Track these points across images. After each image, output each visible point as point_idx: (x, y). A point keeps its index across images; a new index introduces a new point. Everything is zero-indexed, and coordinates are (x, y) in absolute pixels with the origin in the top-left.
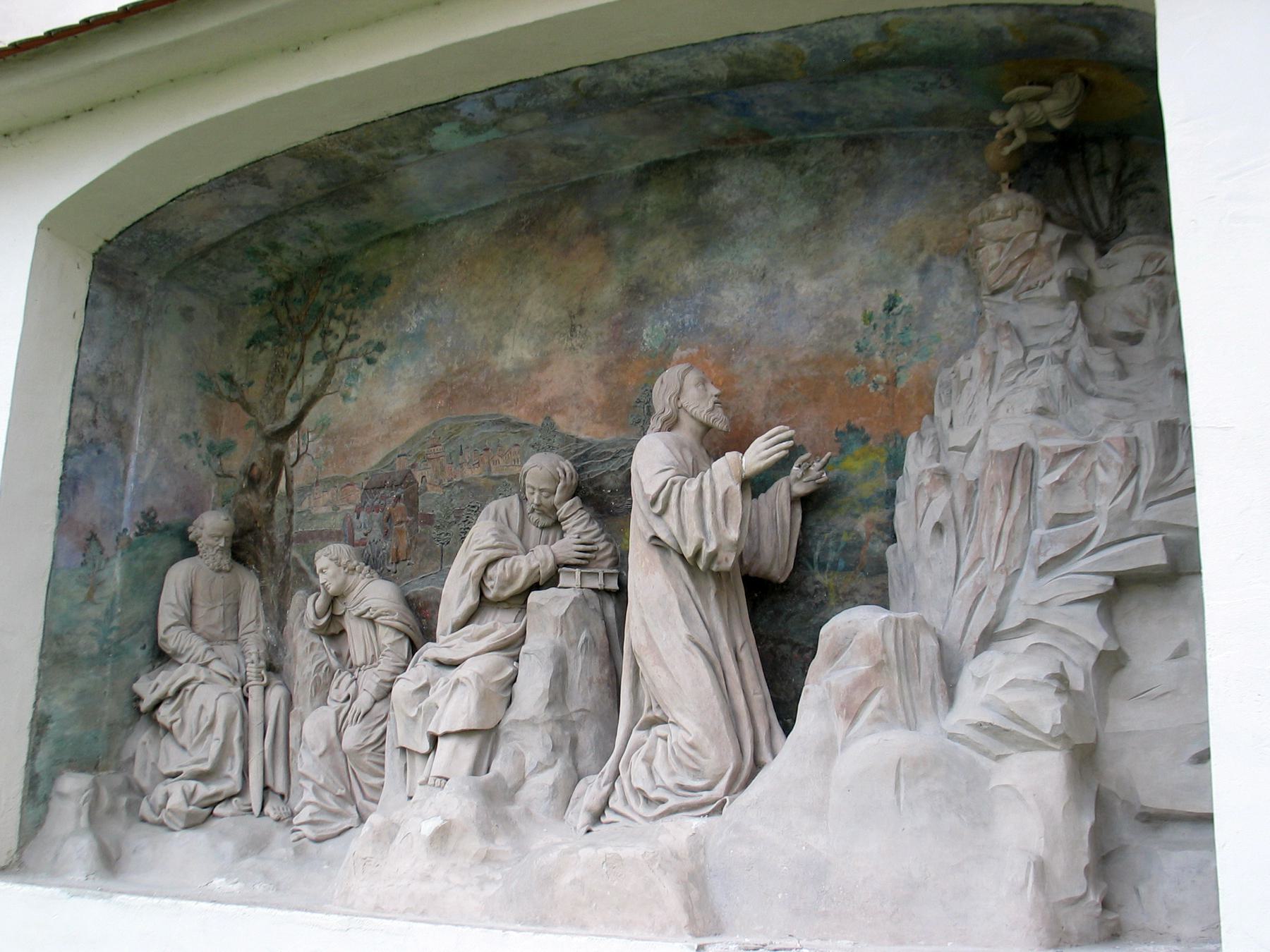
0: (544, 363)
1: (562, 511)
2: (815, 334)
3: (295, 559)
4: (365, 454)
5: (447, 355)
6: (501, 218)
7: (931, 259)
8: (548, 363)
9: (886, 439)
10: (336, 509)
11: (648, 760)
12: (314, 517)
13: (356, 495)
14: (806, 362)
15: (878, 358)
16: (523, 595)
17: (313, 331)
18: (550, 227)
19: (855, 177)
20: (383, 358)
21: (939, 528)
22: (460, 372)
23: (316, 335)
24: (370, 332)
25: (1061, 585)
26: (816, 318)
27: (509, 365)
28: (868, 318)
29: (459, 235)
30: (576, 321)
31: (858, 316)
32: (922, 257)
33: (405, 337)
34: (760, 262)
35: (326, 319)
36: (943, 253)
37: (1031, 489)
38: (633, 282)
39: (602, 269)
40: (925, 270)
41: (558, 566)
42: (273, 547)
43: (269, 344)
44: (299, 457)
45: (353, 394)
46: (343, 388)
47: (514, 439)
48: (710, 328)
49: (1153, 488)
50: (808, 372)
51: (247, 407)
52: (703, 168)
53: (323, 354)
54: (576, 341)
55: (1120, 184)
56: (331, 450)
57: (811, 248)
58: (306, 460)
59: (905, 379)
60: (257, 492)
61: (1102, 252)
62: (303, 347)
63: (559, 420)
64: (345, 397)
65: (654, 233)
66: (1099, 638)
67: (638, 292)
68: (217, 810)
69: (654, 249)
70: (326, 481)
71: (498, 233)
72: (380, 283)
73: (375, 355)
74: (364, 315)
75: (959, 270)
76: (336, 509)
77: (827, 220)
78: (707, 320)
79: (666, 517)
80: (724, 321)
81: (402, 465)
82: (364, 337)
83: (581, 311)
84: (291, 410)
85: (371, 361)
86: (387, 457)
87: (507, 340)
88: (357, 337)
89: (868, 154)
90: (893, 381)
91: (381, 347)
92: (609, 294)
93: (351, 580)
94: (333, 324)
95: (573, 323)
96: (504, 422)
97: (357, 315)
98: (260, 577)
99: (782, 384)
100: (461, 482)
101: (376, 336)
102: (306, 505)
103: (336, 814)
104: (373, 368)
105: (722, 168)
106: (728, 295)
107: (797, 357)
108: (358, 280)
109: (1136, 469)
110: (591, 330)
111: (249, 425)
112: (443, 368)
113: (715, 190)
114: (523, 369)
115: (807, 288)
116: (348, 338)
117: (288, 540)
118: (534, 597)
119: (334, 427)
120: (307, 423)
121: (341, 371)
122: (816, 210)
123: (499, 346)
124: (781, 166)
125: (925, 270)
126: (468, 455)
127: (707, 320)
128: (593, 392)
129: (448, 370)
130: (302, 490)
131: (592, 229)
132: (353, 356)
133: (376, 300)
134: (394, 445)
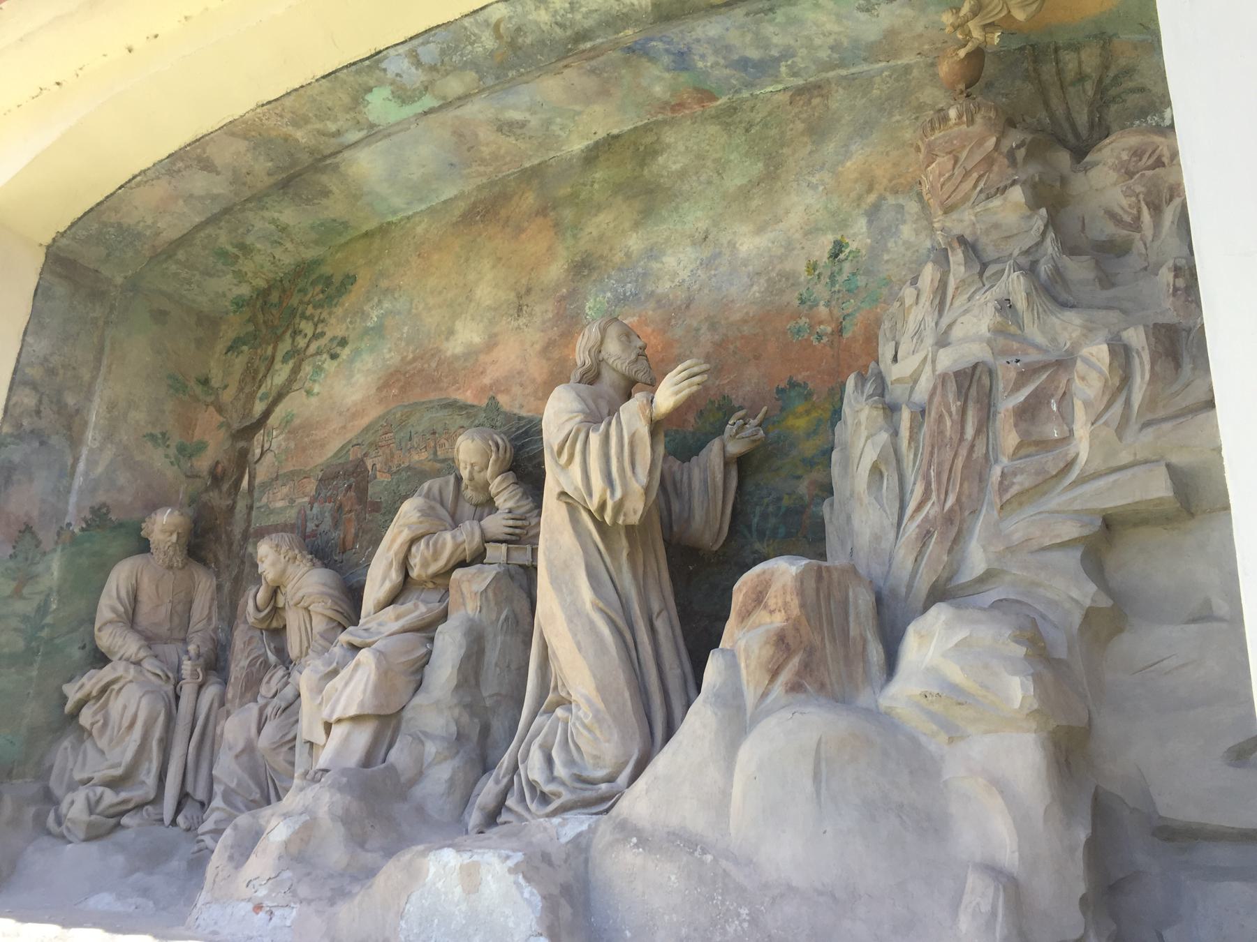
0: (491, 343)
1: (493, 489)
4: (323, 446)
7: (882, 198)
8: (496, 344)
10: (292, 501)
12: (272, 512)
13: (311, 486)
14: (745, 321)
15: (822, 310)
16: (447, 573)
17: (284, 332)
18: (503, 213)
20: (345, 353)
22: (415, 359)
23: (288, 336)
28: (812, 267)
30: (523, 302)
31: (802, 267)
32: (872, 198)
33: (366, 331)
34: (703, 225)
35: (297, 320)
36: (895, 192)
38: (578, 258)
39: (549, 248)
42: (231, 545)
43: (245, 348)
44: (262, 454)
45: (316, 389)
46: (307, 385)
49: (1151, 402)
50: (746, 330)
51: (220, 410)
54: (522, 321)
56: (292, 445)
57: (755, 203)
58: (269, 457)
62: (275, 348)
63: (503, 400)
65: (599, 208)
66: (1085, 592)
68: (125, 820)
70: (285, 475)
71: (455, 224)
73: (338, 350)
74: (330, 314)
75: (913, 207)
76: (292, 501)
77: (772, 173)
80: (664, 287)
82: (329, 335)
83: (529, 291)
84: (259, 408)
85: (334, 357)
86: (342, 448)
87: (459, 325)
88: (323, 334)
90: (840, 331)
91: (343, 342)
92: (555, 271)
96: (452, 405)
99: (720, 345)
100: (409, 468)
101: (340, 331)
102: (264, 500)
104: (335, 363)
106: (670, 261)
107: (737, 316)
108: (328, 281)
109: (1126, 380)
113: (661, 160)
114: (472, 353)
116: (316, 336)
117: (245, 536)
118: (457, 574)
119: (297, 422)
120: (273, 420)
121: (307, 368)
122: (760, 165)
123: (451, 332)
125: (873, 213)
127: (649, 288)
129: (403, 359)
131: (542, 212)
132: (319, 352)
134: (349, 436)
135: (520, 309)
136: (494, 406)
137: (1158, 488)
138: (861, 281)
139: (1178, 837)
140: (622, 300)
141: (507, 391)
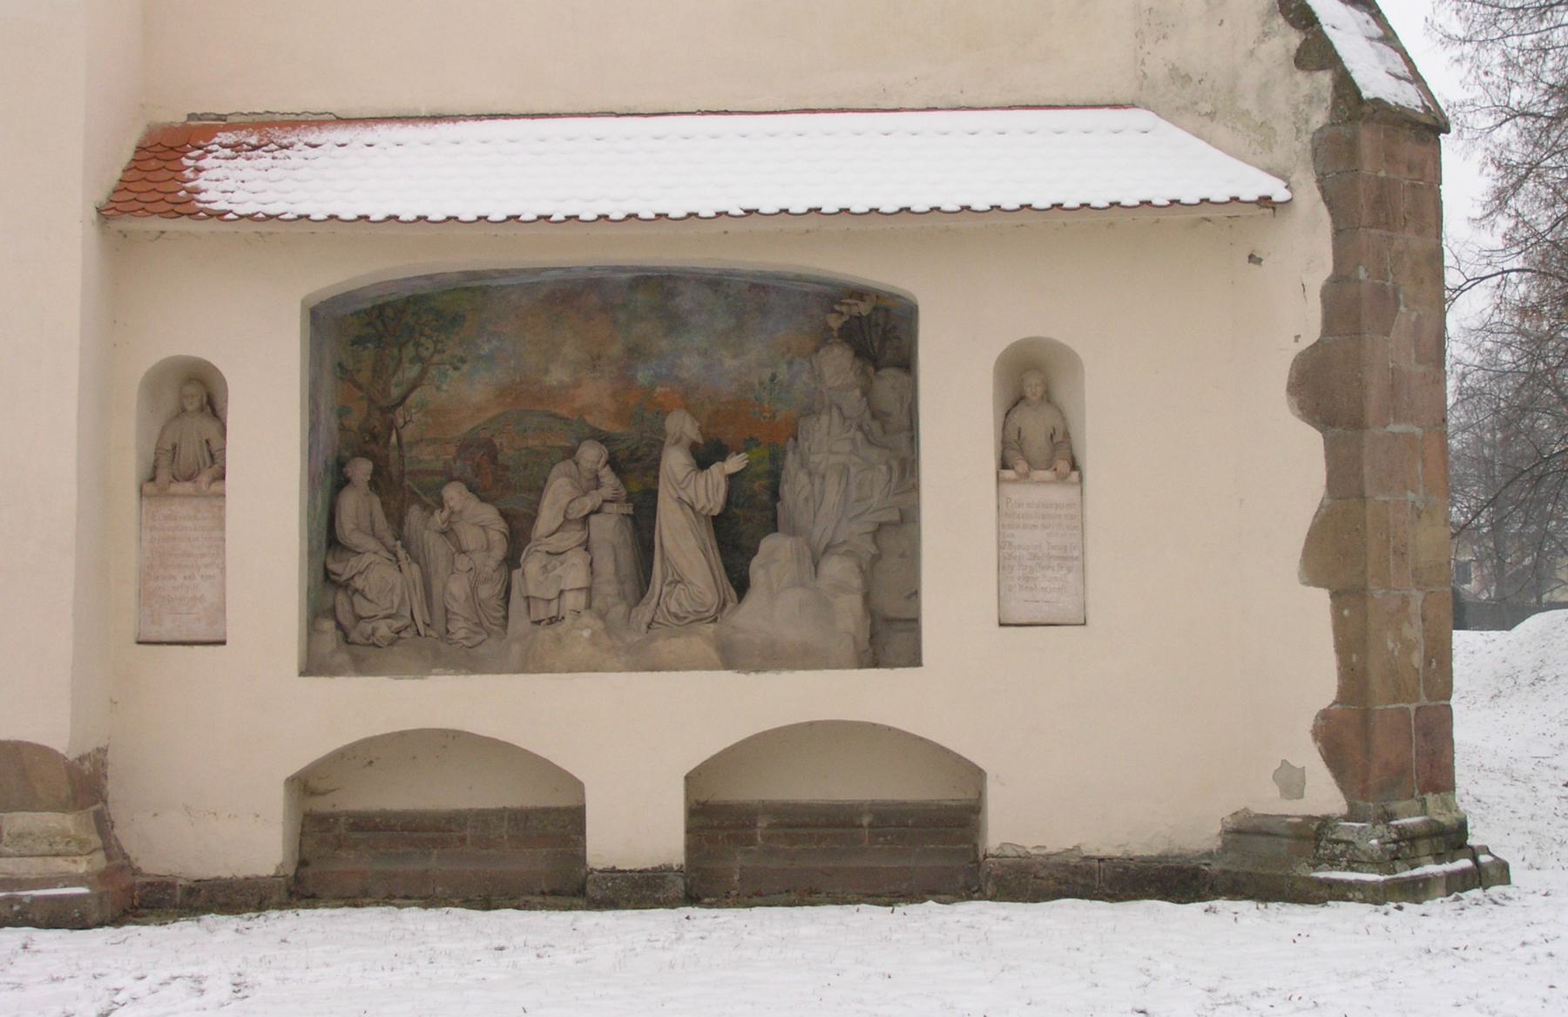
0: (577, 384)
12: (420, 462)
13: (452, 449)
16: (587, 517)
20: (465, 368)
28: (761, 383)
32: (789, 356)
40: (790, 363)
45: (444, 387)
51: (359, 387)
53: (418, 358)
58: (410, 426)
59: (779, 417)
61: (877, 369)
64: (438, 388)
66: (873, 550)
67: (635, 352)
75: (807, 365)
83: (599, 357)
84: (395, 392)
85: (456, 368)
90: (774, 417)
91: (463, 361)
92: (616, 349)
94: (423, 340)
95: (594, 362)
96: (554, 416)
98: (380, 495)
101: (459, 352)
103: (476, 633)
106: (686, 360)
115: (730, 363)
117: (402, 474)
118: (593, 518)
121: (433, 372)
123: (547, 371)
125: (790, 363)
130: (411, 445)
137: (896, 516)
139: (889, 621)
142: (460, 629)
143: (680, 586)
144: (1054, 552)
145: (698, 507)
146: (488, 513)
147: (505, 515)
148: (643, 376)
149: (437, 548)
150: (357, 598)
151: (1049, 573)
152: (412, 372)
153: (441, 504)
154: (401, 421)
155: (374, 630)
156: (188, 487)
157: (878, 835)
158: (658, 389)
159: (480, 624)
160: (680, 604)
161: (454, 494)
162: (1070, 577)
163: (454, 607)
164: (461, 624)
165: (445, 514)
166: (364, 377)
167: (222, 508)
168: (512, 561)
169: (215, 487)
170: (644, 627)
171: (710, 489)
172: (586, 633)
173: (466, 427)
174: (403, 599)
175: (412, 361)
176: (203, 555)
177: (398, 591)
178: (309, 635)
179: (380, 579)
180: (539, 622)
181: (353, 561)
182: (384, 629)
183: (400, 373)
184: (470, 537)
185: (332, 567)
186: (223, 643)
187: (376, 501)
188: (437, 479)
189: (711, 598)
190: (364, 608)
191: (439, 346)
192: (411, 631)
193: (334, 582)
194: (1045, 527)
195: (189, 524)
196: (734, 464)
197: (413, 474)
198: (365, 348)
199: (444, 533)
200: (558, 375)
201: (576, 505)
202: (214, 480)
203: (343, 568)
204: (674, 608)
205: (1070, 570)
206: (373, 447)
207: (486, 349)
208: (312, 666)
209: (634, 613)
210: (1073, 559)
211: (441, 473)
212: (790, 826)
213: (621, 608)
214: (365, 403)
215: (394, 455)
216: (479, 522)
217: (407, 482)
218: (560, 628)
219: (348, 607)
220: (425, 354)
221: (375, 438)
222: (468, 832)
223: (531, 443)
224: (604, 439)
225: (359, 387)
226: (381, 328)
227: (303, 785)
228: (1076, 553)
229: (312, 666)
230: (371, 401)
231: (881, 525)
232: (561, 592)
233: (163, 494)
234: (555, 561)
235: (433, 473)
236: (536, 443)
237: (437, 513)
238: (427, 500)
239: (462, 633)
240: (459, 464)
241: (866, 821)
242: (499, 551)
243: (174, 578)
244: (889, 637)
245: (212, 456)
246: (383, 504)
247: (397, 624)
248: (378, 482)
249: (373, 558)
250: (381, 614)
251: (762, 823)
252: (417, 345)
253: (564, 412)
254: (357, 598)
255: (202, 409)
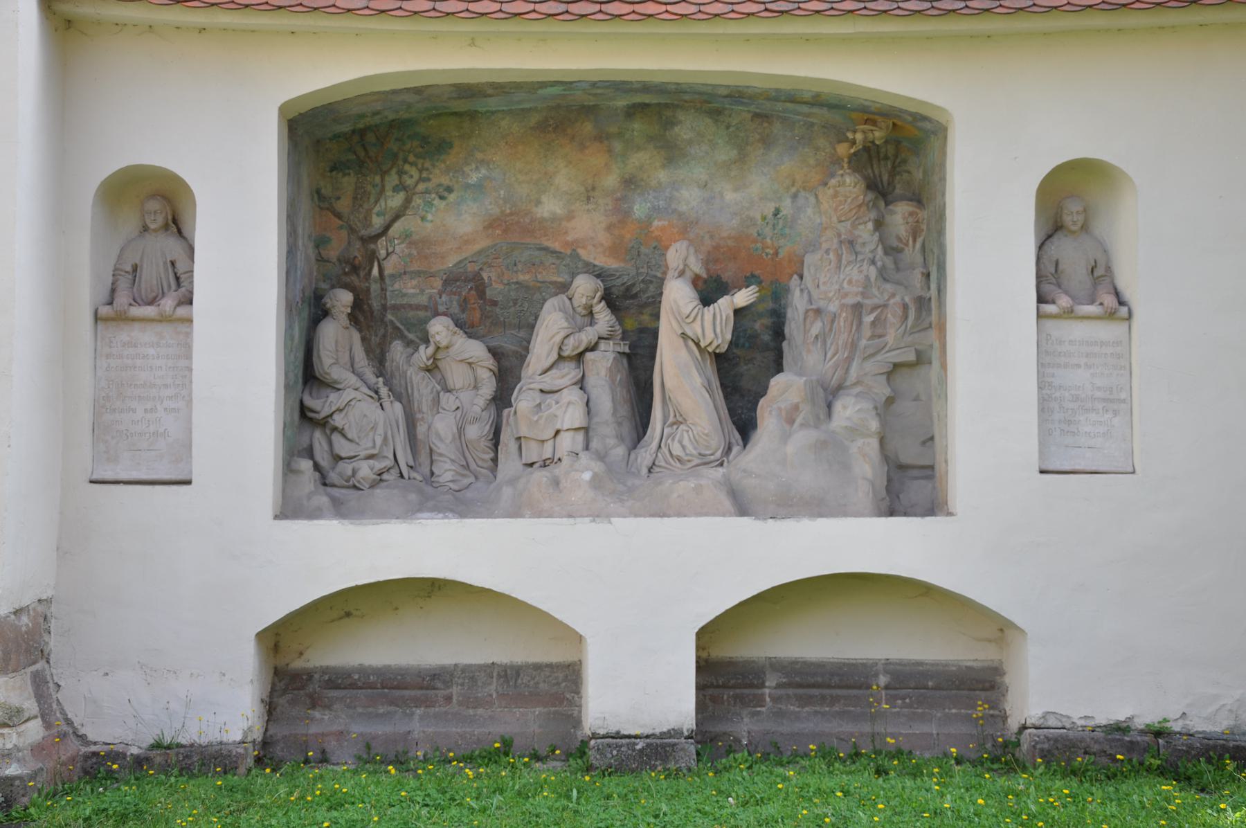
0: (570, 216)
1: (597, 309)
2: (735, 222)
3: (392, 322)
4: (443, 258)
5: (501, 202)
6: (534, 119)
7: (798, 191)
8: (573, 217)
9: (772, 283)
10: (422, 291)
11: (680, 442)
12: (405, 295)
13: (438, 283)
14: (729, 238)
15: (768, 240)
16: (581, 354)
17: (391, 169)
18: (569, 131)
19: (758, 137)
20: (452, 197)
21: (817, 337)
22: (511, 214)
23: (394, 171)
24: (439, 177)
25: (870, 366)
26: (736, 214)
27: (546, 215)
28: (764, 218)
29: (504, 123)
30: (591, 194)
31: (758, 217)
32: (794, 190)
34: (704, 177)
35: (400, 162)
36: (804, 189)
37: (860, 323)
38: (627, 176)
39: (606, 165)
40: (795, 196)
41: (600, 338)
42: (372, 312)
44: (388, 254)
45: (429, 217)
47: (551, 260)
48: (675, 211)
49: (912, 327)
50: (730, 243)
51: (339, 216)
52: (668, 113)
54: (591, 207)
55: (894, 167)
56: (415, 253)
57: (733, 174)
58: (394, 258)
59: (782, 254)
60: (358, 275)
61: (887, 204)
62: (382, 180)
63: (581, 252)
64: (423, 218)
65: (639, 149)
67: (630, 183)
69: (640, 158)
70: (412, 272)
71: (532, 128)
72: (443, 147)
73: (446, 194)
74: (433, 166)
75: (812, 199)
76: (422, 291)
77: (742, 159)
78: (673, 206)
79: (693, 325)
80: (683, 208)
81: (472, 268)
82: (435, 181)
83: (594, 189)
84: (377, 222)
85: (442, 198)
86: (460, 262)
87: (544, 198)
88: (429, 180)
89: (765, 125)
90: (777, 253)
91: (449, 190)
92: (611, 180)
93: (455, 337)
94: (407, 167)
95: (589, 194)
96: (546, 249)
97: (427, 164)
98: (360, 331)
99: (717, 248)
100: (517, 283)
101: (445, 180)
102: (397, 286)
103: (463, 476)
104: (444, 203)
105: (681, 116)
106: (685, 193)
107: (725, 234)
108: (425, 140)
109: (906, 318)
110: (601, 201)
111: (341, 227)
112: (498, 211)
113: (677, 129)
114: (555, 219)
115: (730, 196)
116: (421, 180)
117: (384, 308)
118: (589, 355)
119: (415, 237)
120: (392, 231)
121: (417, 201)
122: (735, 152)
124: (716, 121)
125: (795, 196)
126: (520, 267)
127: (673, 206)
128: (604, 238)
129: (502, 212)
130: (393, 276)
132: (427, 192)
133: (443, 157)
134: (464, 255)
135: (588, 198)
136: (575, 256)
137: (912, 357)
138: (787, 231)
139: (902, 467)
140: (656, 209)
141: (584, 247)
142: (446, 472)
143: (682, 427)
144: (1099, 394)
145: (703, 344)
146: (476, 350)
147: (495, 353)
148: (640, 209)
149: (423, 388)
150: (336, 438)
151: (1093, 416)
152: (396, 201)
153: (426, 341)
154: (383, 253)
155: (354, 472)
156: (149, 311)
157: (896, 697)
158: (656, 223)
159: (467, 467)
160: (684, 447)
161: (440, 328)
162: (1116, 421)
163: (441, 448)
164: (448, 466)
165: (431, 350)
166: (344, 205)
167: (189, 335)
168: (502, 399)
169: (182, 311)
170: (644, 471)
171: (715, 324)
172: (587, 476)
173: (451, 262)
174: (385, 439)
175: (396, 189)
176: (166, 386)
177: (380, 430)
178: (285, 475)
179: (363, 415)
180: (531, 465)
181: (333, 396)
182: (366, 470)
183: (382, 202)
184: (457, 375)
185: (309, 402)
186: (188, 482)
187: (356, 336)
188: (422, 314)
189: (715, 443)
190: (343, 448)
191: (424, 175)
192: (395, 472)
193: (311, 419)
194: (1088, 366)
195: (151, 351)
196: (743, 297)
197: (396, 308)
198: (344, 175)
199: (428, 370)
200: (550, 206)
201: (571, 341)
202: (180, 304)
203: (322, 404)
204: (676, 450)
205: (1116, 413)
206: (354, 278)
207: (474, 178)
208: (289, 509)
209: (633, 456)
210: (1124, 401)
211: (426, 308)
212: (800, 686)
213: (620, 451)
214: (344, 233)
215: (375, 287)
216: (467, 356)
217: (389, 317)
218: (558, 470)
219: (326, 447)
220: (409, 182)
221: (355, 269)
222: (455, 690)
223: (521, 277)
224: (600, 274)
225: (339, 216)
226: (362, 154)
227: (276, 640)
228: (1123, 396)
229: (289, 509)
230: (352, 230)
231: (896, 366)
232: (558, 432)
233: (122, 318)
234: (550, 399)
235: (418, 307)
236: (527, 277)
237: (422, 348)
238: (411, 336)
239: (448, 476)
240: (444, 298)
241: (883, 680)
242: (488, 387)
243: (134, 411)
244: (909, 484)
245: (177, 279)
246: (363, 339)
247: (379, 465)
248: (360, 315)
249: (353, 394)
250: (363, 454)
251: (771, 681)
252: (401, 173)
253: (556, 246)
254: (336, 438)
255: (166, 227)
